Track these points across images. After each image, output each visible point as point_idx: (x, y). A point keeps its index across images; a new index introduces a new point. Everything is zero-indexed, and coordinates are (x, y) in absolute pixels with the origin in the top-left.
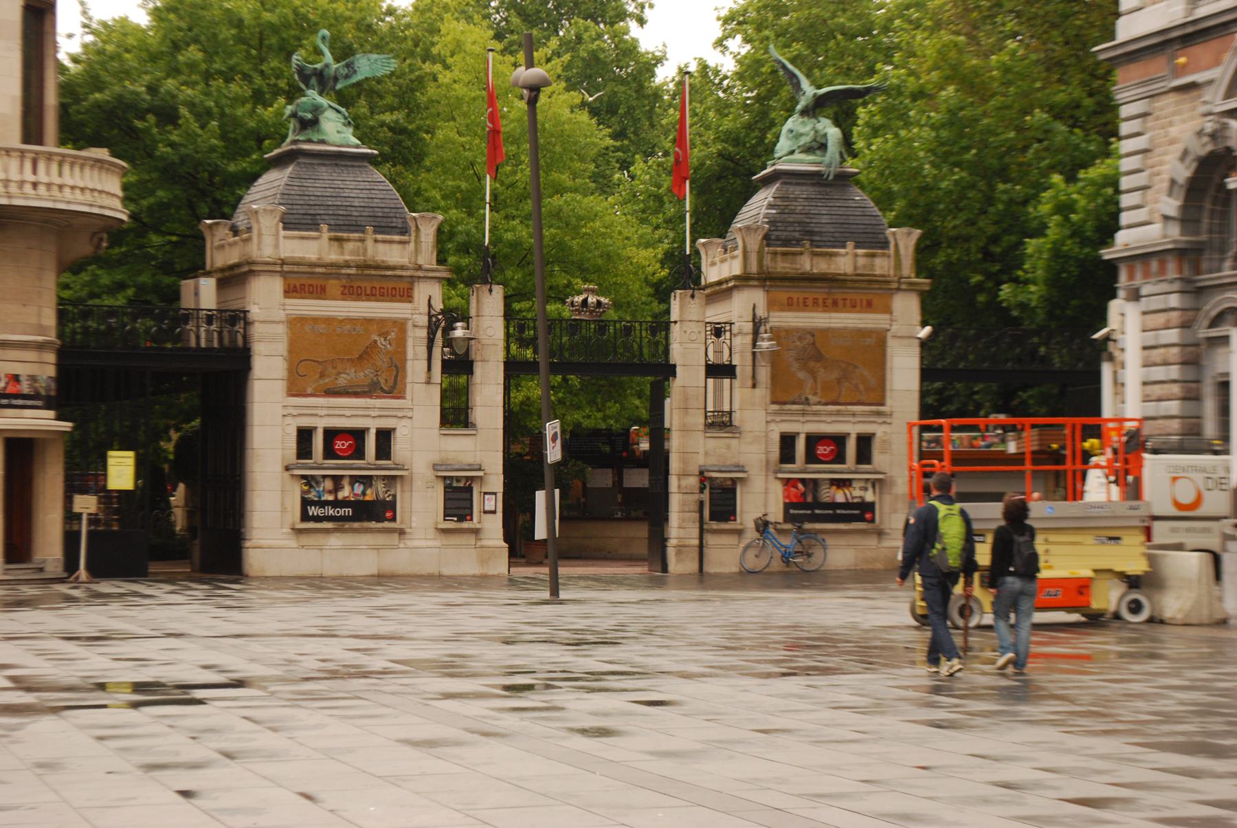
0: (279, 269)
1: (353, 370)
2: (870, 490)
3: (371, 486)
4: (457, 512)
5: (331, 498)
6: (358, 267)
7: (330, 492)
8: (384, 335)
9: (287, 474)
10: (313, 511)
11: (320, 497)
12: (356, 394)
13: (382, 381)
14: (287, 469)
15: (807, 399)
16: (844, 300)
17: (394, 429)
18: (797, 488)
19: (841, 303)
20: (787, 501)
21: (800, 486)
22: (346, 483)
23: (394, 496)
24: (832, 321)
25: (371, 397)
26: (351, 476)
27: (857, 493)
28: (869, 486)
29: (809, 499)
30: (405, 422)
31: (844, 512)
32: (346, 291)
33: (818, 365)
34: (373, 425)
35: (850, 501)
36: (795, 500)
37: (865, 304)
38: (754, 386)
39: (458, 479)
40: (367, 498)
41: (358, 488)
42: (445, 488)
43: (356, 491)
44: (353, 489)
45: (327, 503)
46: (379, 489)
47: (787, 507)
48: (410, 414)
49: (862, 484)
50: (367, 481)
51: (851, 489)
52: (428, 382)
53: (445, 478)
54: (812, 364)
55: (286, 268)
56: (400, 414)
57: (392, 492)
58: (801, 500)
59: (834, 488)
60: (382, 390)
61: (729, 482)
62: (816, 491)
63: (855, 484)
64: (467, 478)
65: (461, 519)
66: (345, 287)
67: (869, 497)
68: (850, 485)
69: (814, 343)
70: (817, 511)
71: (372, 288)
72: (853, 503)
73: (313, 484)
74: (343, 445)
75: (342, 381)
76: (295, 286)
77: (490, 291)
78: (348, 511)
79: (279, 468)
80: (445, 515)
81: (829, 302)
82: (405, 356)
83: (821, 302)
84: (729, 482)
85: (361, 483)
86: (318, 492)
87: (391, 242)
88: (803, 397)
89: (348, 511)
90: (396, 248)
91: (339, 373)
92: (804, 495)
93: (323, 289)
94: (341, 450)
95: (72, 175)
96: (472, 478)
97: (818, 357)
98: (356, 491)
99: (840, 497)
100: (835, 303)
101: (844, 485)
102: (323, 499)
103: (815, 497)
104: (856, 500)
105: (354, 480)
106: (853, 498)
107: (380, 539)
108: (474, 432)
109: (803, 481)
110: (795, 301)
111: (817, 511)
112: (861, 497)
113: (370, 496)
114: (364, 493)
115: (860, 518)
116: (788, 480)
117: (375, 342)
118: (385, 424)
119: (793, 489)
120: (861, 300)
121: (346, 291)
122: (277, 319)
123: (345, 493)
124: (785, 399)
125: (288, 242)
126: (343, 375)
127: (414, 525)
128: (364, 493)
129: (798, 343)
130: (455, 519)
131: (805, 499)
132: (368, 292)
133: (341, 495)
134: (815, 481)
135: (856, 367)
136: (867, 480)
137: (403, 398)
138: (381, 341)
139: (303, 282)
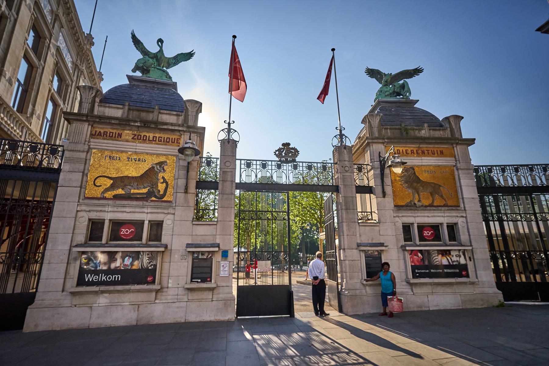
0: (85, 119)
1: (136, 184)
2: (462, 257)
3: (138, 258)
4: (200, 275)
5: (105, 268)
6: (141, 122)
10: (88, 278)
11: (96, 267)
12: (137, 199)
13: (156, 191)
15: (415, 204)
16: (428, 151)
17: (163, 221)
18: (418, 256)
19: (426, 152)
20: (413, 264)
21: (420, 255)
22: (119, 256)
23: (155, 266)
24: (423, 161)
25: (147, 201)
26: (122, 252)
27: (454, 259)
28: (461, 254)
29: (426, 263)
31: (449, 271)
32: (136, 137)
33: (419, 185)
35: (452, 264)
36: (418, 264)
37: (439, 152)
38: (384, 196)
39: (203, 253)
40: (134, 267)
41: (128, 261)
42: (193, 259)
43: (125, 263)
44: (123, 261)
45: (102, 271)
46: (144, 261)
47: (414, 268)
49: (457, 253)
50: (136, 256)
51: (451, 256)
53: (193, 253)
54: (415, 184)
57: (155, 263)
58: (422, 263)
59: (440, 256)
60: (155, 197)
61: (376, 253)
62: (430, 258)
63: (452, 253)
64: (209, 252)
65: (204, 280)
66: (135, 135)
67: (462, 261)
68: (450, 254)
69: (415, 173)
70: (432, 271)
71: (154, 137)
72: (453, 265)
73: (92, 258)
74: (127, 232)
76: (100, 132)
78: (118, 277)
80: (192, 278)
81: (420, 152)
83: (415, 151)
84: (376, 253)
85: (130, 257)
86: (95, 264)
88: (413, 203)
89: (118, 277)
91: (125, 185)
92: (423, 260)
93: (120, 135)
94: (125, 235)
96: (213, 252)
97: (418, 180)
98: (125, 263)
99: (445, 262)
100: (423, 152)
101: (446, 254)
102: (98, 268)
103: (429, 261)
104: (454, 263)
106: (453, 262)
107: (141, 297)
109: (421, 251)
110: (401, 151)
111: (432, 271)
112: (457, 261)
113: (137, 265)
114: (132, 264)
115: (460, 275)
116: (412, 251)
118: (159, 217)
119: (415, 257)
120: (437, 151)
121: (136, 137)
122: (82, 149)
123: (117, 264)
124: (402, 204)
126: (128, 187)
127: (170, 285)
128: (132, 264)
129: (406, 173)
130: (199, 280)
131: (424, 263)
132: (151, 139)
133: (113, 266)
134: (428, 251)
135: (440, 186)
136: (460, 250)
139: (106, 130)
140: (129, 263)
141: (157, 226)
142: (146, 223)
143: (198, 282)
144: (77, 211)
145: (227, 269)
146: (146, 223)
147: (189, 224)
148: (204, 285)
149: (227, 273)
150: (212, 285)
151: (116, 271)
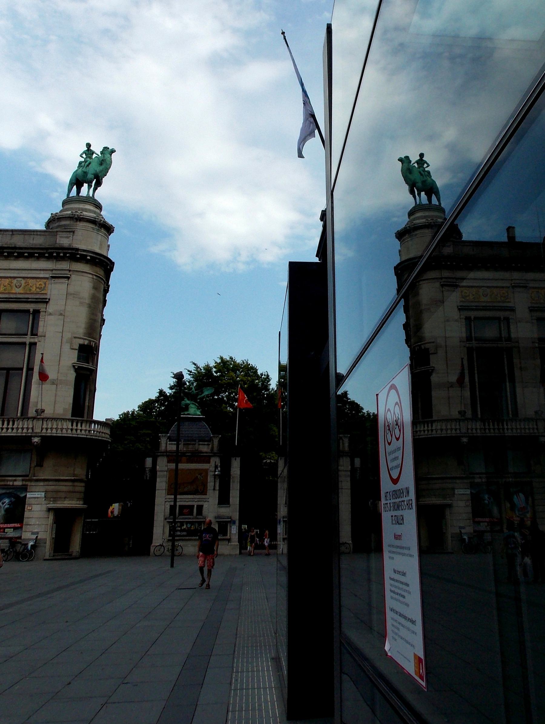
0: (165, 454)
5: (179, 529)
7: (179, 527)
8: (200, 474)
9: (165, 521)
14: (166, 519)
30: (206, 503)
34: (196, 504)
40: (192, 529)
41: (189, 526)
48: (208, 500)
52: (214, 489)
55: (168, 454)
56: (205, 500)
57: (201, 526)
75: (186, 489)
77: (236, 459)
78: (185, 533)
79: (163, 519)
82: (207, 481)
87: (204, 445)
90: (206, 447)
91: (185, 487)
95: (102, 429)
98: (188, 526)
105: (187, 523)
108: (229, 506)
117: (197, 477)
118: (200, 503)
125: (170, 445)
128: (191, 527)
133: (183, 528)
137: (206, 495)
138: (199, 476)
140: (189, 527)
141: (200, 508)
142: (195, 506)
143: (221, 536)
144: (165, 502)
145: (235, 529)
146: (195, 506)
147: (216, 506)
148: (224, 537)
149: (235, 532)
150: (228, 537)
151: (184, 530)
